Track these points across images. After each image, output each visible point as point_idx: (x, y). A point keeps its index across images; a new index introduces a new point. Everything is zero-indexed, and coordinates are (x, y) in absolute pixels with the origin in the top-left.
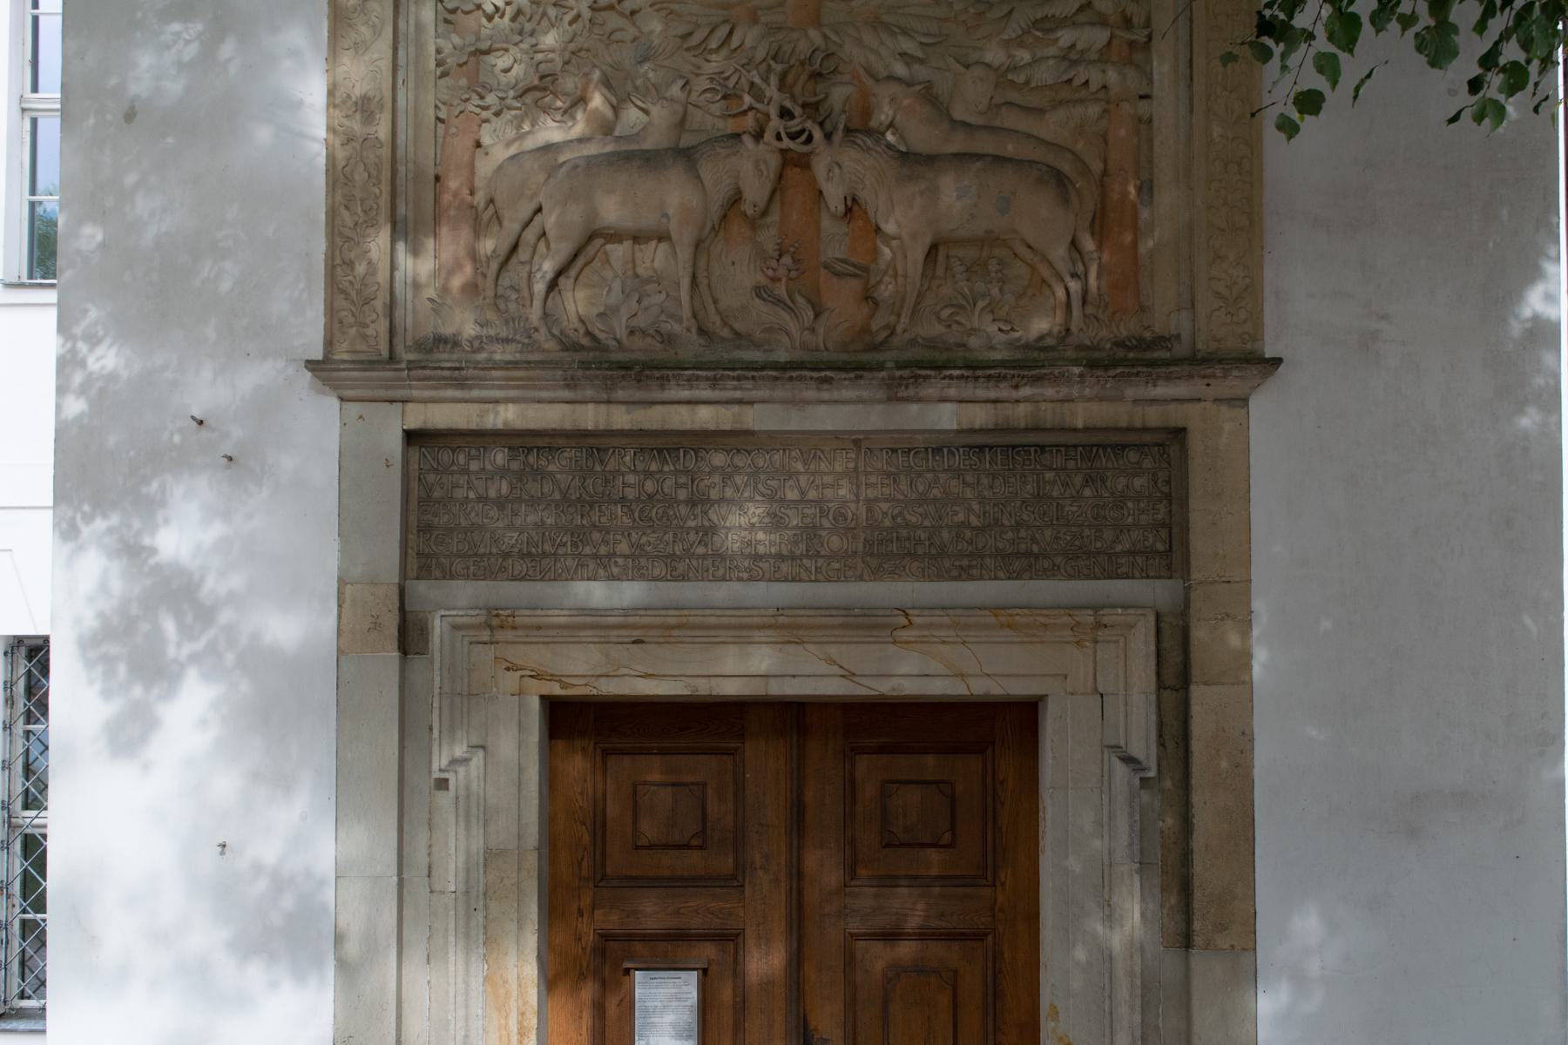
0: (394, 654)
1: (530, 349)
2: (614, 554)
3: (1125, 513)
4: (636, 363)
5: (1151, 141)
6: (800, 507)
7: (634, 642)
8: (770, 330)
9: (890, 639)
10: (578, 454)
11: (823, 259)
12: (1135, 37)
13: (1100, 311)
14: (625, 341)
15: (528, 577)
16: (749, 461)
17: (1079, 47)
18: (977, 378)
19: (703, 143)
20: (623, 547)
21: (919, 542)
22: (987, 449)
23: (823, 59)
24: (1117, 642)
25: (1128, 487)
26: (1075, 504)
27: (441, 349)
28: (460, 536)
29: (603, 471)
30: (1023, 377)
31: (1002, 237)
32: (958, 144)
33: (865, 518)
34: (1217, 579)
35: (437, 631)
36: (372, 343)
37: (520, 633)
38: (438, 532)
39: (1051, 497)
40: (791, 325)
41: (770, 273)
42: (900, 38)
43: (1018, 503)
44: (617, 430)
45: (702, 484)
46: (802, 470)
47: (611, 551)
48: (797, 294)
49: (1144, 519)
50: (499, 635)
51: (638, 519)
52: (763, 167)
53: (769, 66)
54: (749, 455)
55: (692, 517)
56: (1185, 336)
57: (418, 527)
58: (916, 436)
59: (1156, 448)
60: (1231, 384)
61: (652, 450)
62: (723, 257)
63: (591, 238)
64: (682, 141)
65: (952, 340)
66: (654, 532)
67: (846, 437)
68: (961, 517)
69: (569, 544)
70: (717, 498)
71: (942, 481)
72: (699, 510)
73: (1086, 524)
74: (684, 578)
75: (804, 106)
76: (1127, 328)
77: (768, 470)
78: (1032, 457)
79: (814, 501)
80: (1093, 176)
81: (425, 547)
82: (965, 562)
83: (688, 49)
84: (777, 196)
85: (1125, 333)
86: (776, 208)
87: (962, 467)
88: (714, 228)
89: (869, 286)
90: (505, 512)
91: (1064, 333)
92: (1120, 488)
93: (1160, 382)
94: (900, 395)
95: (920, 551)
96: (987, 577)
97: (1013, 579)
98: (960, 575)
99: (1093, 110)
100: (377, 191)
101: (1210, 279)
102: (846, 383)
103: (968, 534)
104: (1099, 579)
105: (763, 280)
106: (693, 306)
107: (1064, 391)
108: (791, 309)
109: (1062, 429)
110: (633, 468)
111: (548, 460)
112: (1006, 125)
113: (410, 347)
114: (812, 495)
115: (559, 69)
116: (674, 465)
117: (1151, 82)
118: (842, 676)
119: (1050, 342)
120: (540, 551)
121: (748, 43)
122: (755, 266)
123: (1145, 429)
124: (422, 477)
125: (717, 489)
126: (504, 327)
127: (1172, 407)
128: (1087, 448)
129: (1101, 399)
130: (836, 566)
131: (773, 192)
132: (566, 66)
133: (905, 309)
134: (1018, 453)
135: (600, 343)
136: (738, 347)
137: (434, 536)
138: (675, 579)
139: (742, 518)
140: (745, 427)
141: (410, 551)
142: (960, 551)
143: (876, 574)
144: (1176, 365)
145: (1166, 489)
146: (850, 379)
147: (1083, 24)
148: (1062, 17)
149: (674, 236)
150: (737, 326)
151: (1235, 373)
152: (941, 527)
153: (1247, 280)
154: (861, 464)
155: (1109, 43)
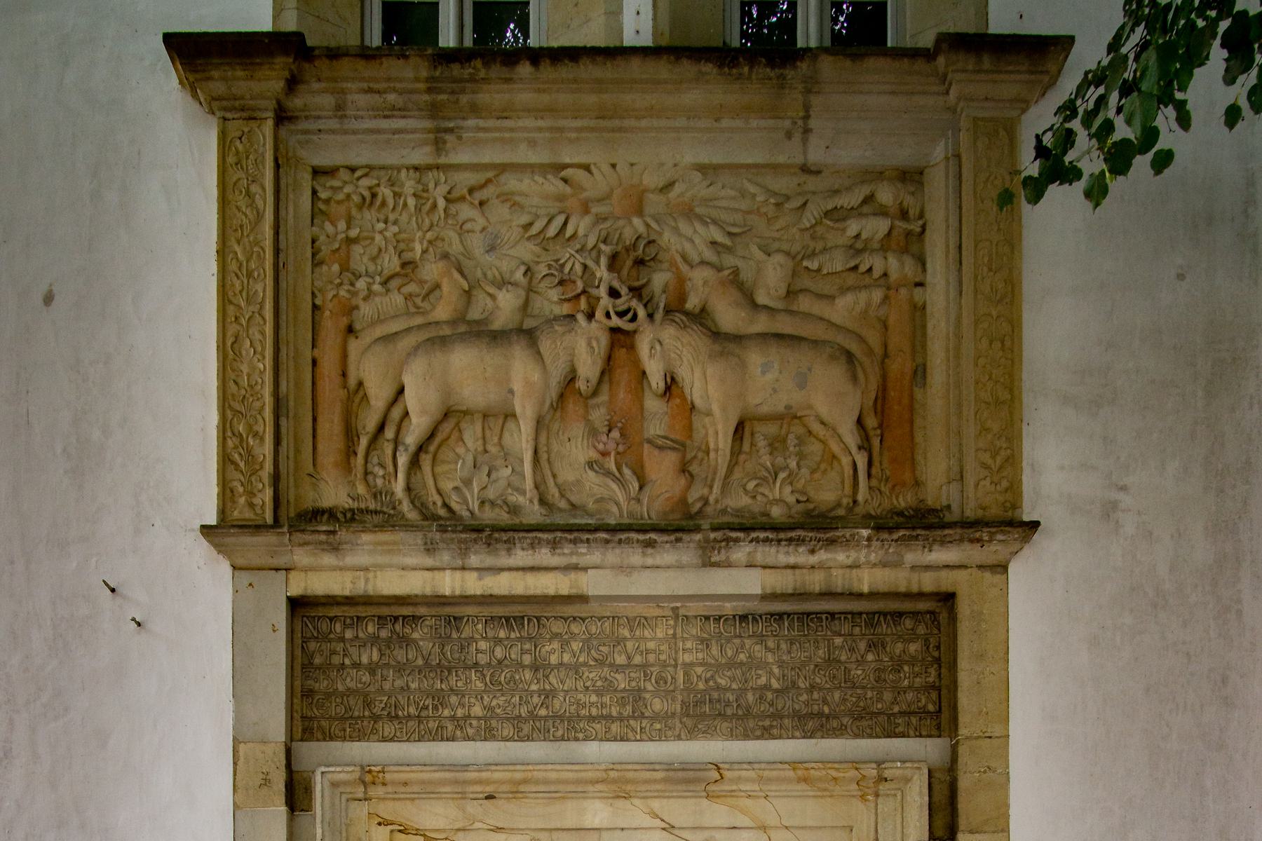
2: (469, 716)
7: (487, 798)
8: (600, 500)
9: (705, 794)
10: (438, 623)
13: (882, 484)
15: (396, 739)
16: (584, 628)
20: (477, 710)
21: (728, 704)
22: (785, 617)
24: (895, 795)
25: (904, 651)
26: (860, 668)
28: (338, 700)
29: (459, 638)
32: (762, 324)
34: (981, 734)
35: (318, 788)
37: (390, 789)
39: (839, 661)
40: (619, 494)
41: (601, 447)
42: (712, 227)
43: (812, 667)
46: (629, 637)
47: (467, 714)
50: (372, 792)
55: (536, 681)
56: (955, 507)
60: (993, 551)
61: (501, 618)
62: (561, 433)
63: (446, 415)
64: (525, 322)
66: (502, 695)
68: (763, 681)
69: (431, 706)
70: (556, 663)
71: (747, 647)
74: (529, 738)
75: (631, 289)
76: (904, 501)
77: (600, 636)
78: (824, 624)
79: (639, 666)
82: (767, 723)
84: (606, 378)
85: (903, 504)
86: (605, 387)
87: (764, 633)
88: (552, 404)
90: (376, 678)
92: (898, 652)
95: (729, 712)
96: (785, 736)
97: (807, 738)
98: (763, 734)
103: (770, 696)
104: (880, 737)
105: (593, 455)
108: (619, 480)
109: (851, 594)
110: (484, 635)
111: (411, 626)
113: (293, 518)
114: (637, 660)
116: (520, 633)
117: (924, 270)
118: (664, 829)
120: (406, 713)
122: (588, 443)
123: (921, 595)
124: (304, 645)
125: (556, 655)
127: (944, 574)
128: (871, 616)
129: (884, 566)
130: (658, 726)
131: (603, 373)
137: (315, 701)
138: (521, 740)
139: (578, 682)
141: (295, 714)
142: (763, 711)
143: (692, 734)
147: (866, 215)
148: (849, 207)
152: (746, 689)
154: (679, 631)
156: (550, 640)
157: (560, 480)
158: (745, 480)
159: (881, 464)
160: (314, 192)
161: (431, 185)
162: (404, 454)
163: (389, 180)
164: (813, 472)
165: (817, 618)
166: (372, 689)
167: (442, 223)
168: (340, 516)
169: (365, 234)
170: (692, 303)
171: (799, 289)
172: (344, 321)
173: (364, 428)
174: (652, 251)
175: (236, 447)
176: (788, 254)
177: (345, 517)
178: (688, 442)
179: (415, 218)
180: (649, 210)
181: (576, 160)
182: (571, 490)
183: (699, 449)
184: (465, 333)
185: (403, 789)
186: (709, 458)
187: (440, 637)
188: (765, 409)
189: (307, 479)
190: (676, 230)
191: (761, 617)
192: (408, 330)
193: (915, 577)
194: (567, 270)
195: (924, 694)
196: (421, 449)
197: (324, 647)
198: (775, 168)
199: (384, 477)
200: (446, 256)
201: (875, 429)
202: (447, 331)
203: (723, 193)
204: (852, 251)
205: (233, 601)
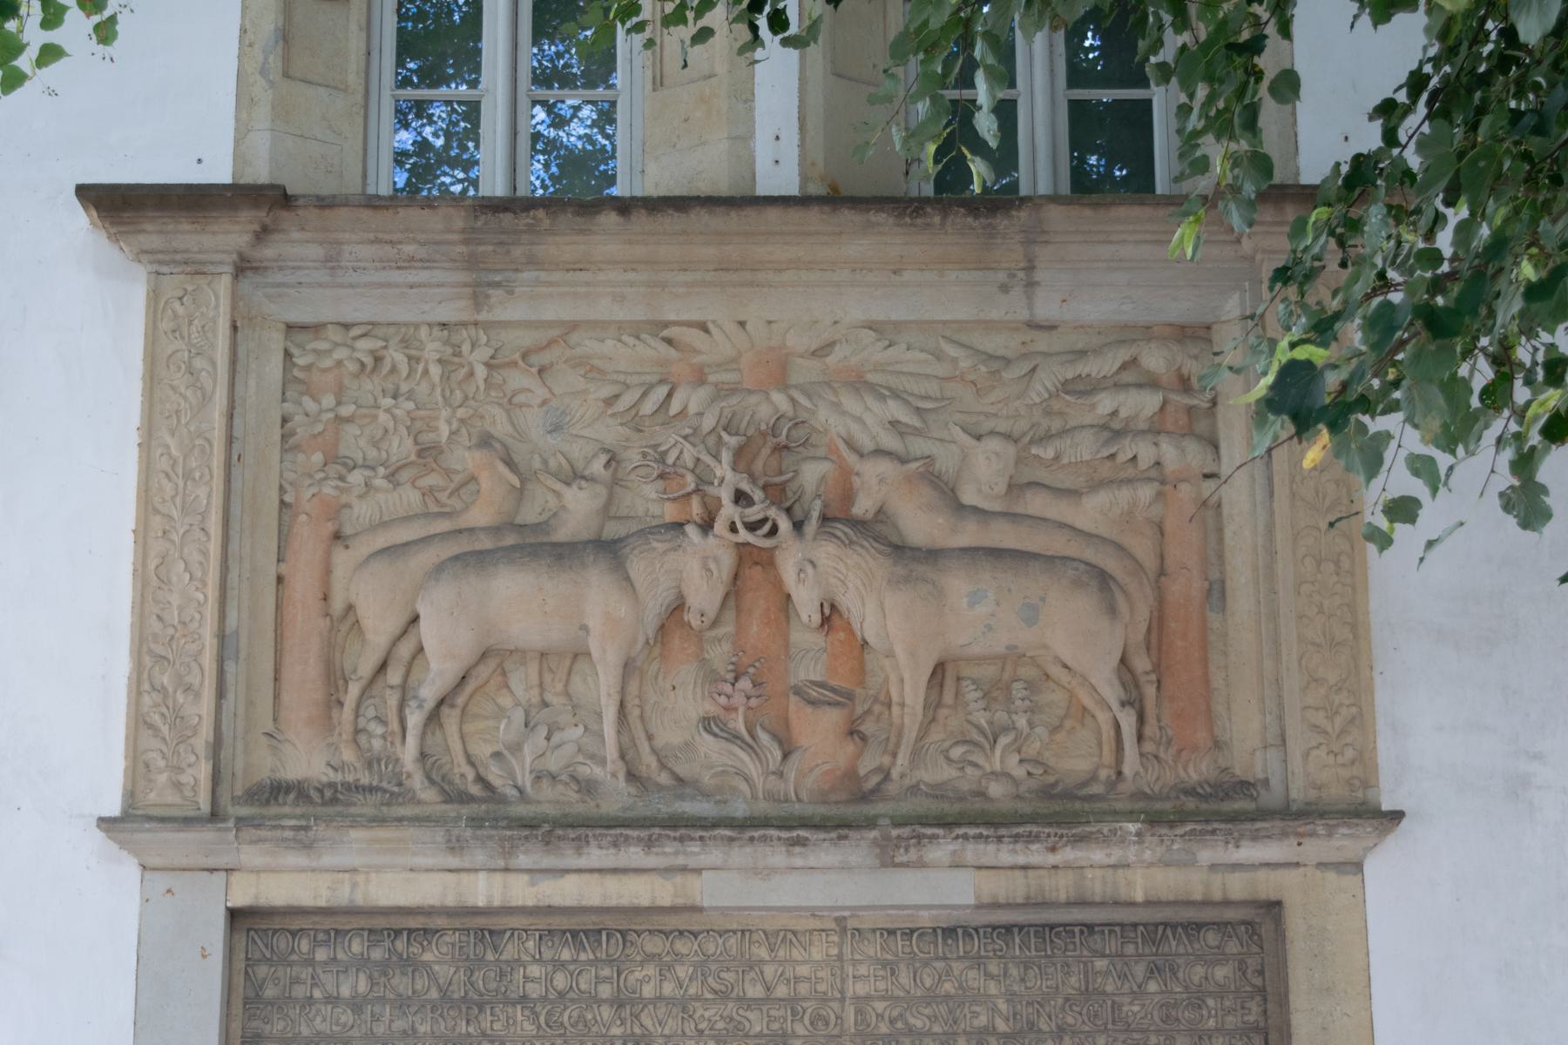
1: (401, 800)
3: (1205, 1012)
4: (545, 819)
5: (1220, 530)
6: (765, 1008)
10: (464, 938)
11: (793, 681)
12: (1195, 402)
13: (1162, 749)
14: (529, 789)
16: (696, 947)
17: (1123, 414)
18: (1000, 839)
19: (633, 534)
22: (1016, 930)
23: (789, 429)
25: (1206, 978)
27: (280, 800)
29: (497, 960)
30: (1062, 836)
31: (1028, 654)
32: (969, 535)
33: (852, 1021)
36: (188, 793)
39: (1104, 993)
42: (891, 403)
43: (1060, 1001)
44: (517, 907)
45: (631, 978)
46: (767, 958)
48: (758, 728)
49: (1231, 1022)
51: (544, 1025)
52: (712, 566)
53: (720, 437)
54: (696, 938)
55: (618, 1022)
56: (1275, 782)
58: (922, 913)
59: (1243, 928)
60: (1342, 843)
61: (564, 932)
62: (660, 678)
63: (484, 656)
65: (965, 787)
67: (826, 913)
68: (983, 1020)
71: (956, 973)
72: (628, 1012)
73: (1152, 1028)
75: (765, 488)
76: (1198, 770)
78: (1077, 940)
80: (1146, 573)
83: (613, 415)
84: (731, 603)
85: (1195, 777)
86: (730, 615)
87: (983, 953)
88: (647, 642)
89: (855, 717)
90: (363, 1017)
91: (1114, 777)
92: (1196, 979)
93: (1243, 843)
94: (897, 860)
99: (1146, 492)
100: (201, 597)
101: (1306, 708)
102: (826, 844)
105: (710, 708)
106: (620, 743)
107: (1116, 854)
111: (422, 945)
112: (1030, 511)
113: (239, 798)
114: (781, 991)
115: (444, 440)
119: (1097, 789)
121: (692, 409)
123: (1227, 903)
124: (250, 970)
125: (652, 983)
126: (366, 772)
127: (1262, 874)
129: (1168, 865)
131: (727, 596)
132: (454, 437)
133: (903, 747)
134: (1058, 935)
135: (494, 792)
136: (681, 797)
139: (686, 1024)
140: (689, 902)
144: (1264, 820)
145: (1258, 981)
146: (832, 839)
147: (1127, 386)
148: (1101, 375)
149: (595, 653)
150: (678, 770)
151: (1345, 831)
152: (955, 1034)
153: (1354, 710)
154: (847, 950)
155: (1162, 409)
156: (642, 964)
157: (659, 742)
158: (947, 744)
159: (1159, 720)
160: (288, 354)
161: (466, 348)
162: (417, 711)
163: (402, 341)
164: (1055, 730)
165: (1066, 932)
166: (355, 1033)
167: (481, 397)
168: (312, 793)
169: (364, 411)
170: (863, 506)
171: (1026, 481)
172: (330, 527)
173: (355, 671)
174: (800, 433)
175: (156, 705)
176: (1007, 436)
177: (323, 797)
178: (859, 691)
179: (439, 390)
180: (795, 378)
181: (685, 317)
182: (676, 757)
183: (876, 700)
184: (513, 548)
186: (890, 713)
187: (468, 959)
188: (976, 650)
189: (264, 739)
190: (837, 406)
191: (976, 930)
192: (426, 540)
193: (1217, 880)
194: (670, 460)
195: (1241, 1039)
196: (441, 702)
197: (280, 973)
198: (989, 326)
199: (384, 737)
200: (485, 441)
201: (1147, 673)
202: (486, 543)
203: (909, 355)
204: (1106, 434)
205: (141, 915)
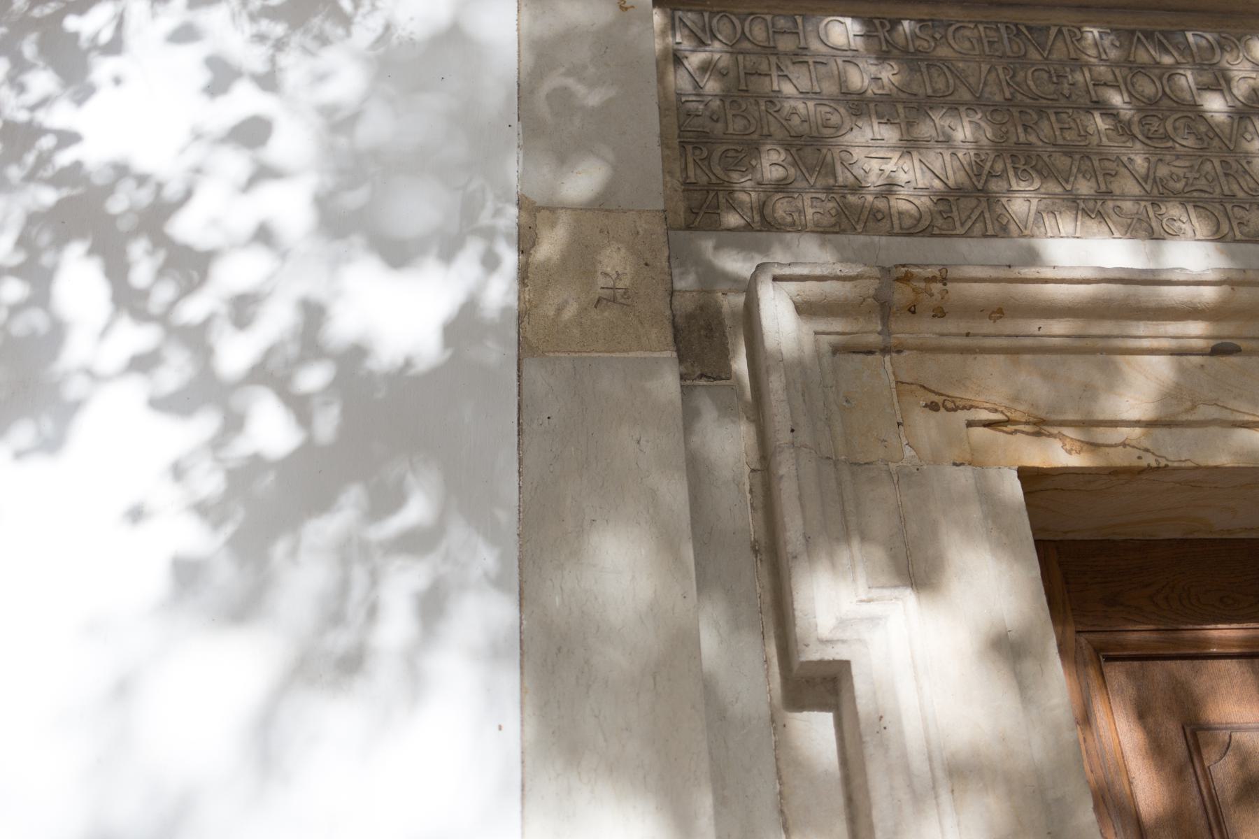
0: (667, 354)
10: (992, 33)
37: (950, 325)
38: (725, 147)
50: (906, 330)
57: (679, 137)
81: (699, 171)
185: (988, 327)
